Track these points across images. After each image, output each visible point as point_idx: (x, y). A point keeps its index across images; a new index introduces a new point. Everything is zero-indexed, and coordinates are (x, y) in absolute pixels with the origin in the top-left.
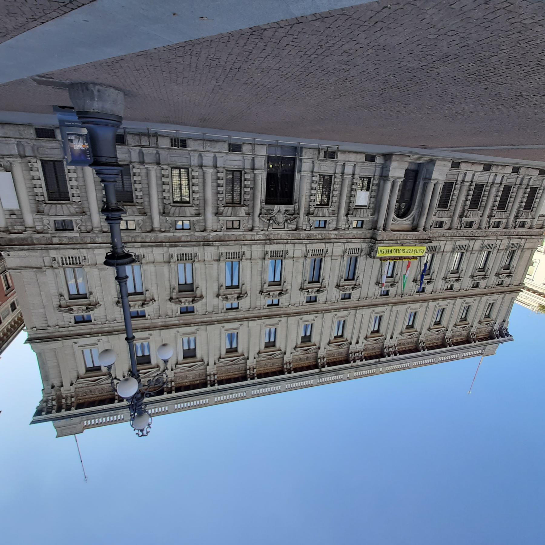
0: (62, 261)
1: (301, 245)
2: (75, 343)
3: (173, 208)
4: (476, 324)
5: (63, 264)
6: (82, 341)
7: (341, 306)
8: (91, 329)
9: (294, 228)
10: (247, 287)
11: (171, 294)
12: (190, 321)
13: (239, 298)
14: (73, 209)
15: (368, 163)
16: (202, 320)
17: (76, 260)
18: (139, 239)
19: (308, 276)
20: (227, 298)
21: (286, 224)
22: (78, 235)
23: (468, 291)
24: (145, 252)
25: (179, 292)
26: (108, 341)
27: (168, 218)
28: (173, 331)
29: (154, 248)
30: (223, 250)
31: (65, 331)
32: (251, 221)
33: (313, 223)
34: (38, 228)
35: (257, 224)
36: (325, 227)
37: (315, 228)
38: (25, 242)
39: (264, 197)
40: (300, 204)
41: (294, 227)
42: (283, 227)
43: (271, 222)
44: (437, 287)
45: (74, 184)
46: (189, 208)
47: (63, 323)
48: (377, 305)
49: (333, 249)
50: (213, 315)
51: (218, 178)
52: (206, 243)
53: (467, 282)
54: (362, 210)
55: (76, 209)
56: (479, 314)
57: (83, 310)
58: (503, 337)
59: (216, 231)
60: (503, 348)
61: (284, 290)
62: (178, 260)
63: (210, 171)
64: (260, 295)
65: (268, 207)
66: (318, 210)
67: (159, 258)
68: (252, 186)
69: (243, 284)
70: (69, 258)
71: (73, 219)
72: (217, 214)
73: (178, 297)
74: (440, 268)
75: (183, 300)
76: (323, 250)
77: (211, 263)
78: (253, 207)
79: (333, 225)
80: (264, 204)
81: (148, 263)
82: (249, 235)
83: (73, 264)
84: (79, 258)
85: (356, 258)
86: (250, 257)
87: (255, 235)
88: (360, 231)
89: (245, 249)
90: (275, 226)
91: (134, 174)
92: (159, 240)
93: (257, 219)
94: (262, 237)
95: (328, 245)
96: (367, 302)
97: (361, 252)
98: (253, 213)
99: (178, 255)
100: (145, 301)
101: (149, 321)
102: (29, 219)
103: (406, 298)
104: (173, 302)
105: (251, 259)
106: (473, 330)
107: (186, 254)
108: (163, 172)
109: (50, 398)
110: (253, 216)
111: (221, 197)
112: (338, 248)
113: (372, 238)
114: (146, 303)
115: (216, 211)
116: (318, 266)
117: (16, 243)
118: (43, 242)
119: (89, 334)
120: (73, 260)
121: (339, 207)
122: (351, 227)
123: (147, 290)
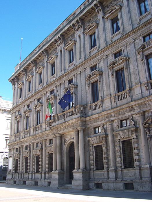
15: (100, 182)
36: (121, 121)
37: (128, 119)
40: (145, 138)
54: (96, 143)
58: (12, 80)
60: (12, 73)
66: (128, 135)
76: (119, 101)
116: (120, 85)
121: (114, 141)
122: (101, 126)
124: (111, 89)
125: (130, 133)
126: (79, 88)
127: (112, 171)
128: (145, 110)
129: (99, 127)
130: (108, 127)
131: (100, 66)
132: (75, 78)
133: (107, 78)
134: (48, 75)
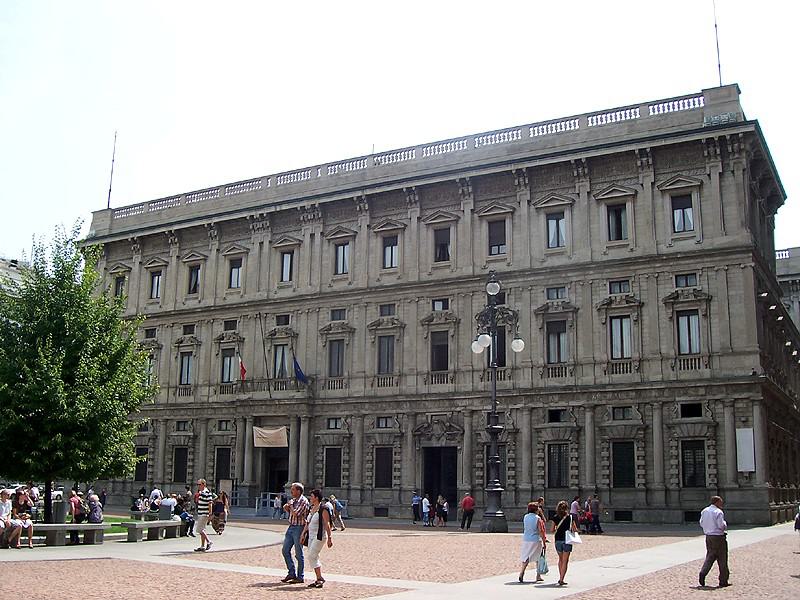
1: (408, 392)
4: (136, 268)
6: (690, 245)
14: (677, 432)
16: (536, 278)
18: (609, 396)
23: (158, 323)
25: (564, 322)
28: (574, 260)
29: (592, 383)
30: (508, 383)
32: (474, 424)
34: (721, 406)
35: (467, 420)
36: (379, 418)
38: (734, 388)
39: (459, 456)
41: (419, 418)
44: (208, 329)
45: (674, 462)
48: (291, 300)
51: (514, 477)
52: (531, 394)
53: (167, 337)
56: (134, 284)
63: (524, 485)
65: (453, 444)
67: (588, 370)
72: (516, 432)
74: (208, 359)
75: (560, 309)
78: (472, 443)
79: (367, 422)
81: (601, 363)
82: (477, 405)
86: (475, 373)
87: (469, 405)
88: (330, 414)
90: (444, 419)
91: (608, 476)
92: (586, 395)
95: (372, 393)
96: (306, 306)
101: (606, 276)
102: (726, 418)
103: (251, 312)
105: (473, 371)
106: (137, 258)
108: (576, 481)
109: (737, 156)
110: (472, 430)
111: (511, 454)
112: (358, 388)
113: (314, 405)
124: (367, 362)
126: (302, 340)
127: (356, 489)
129: (336, 419)
130: (356, 423)
131: (350, 317)
132: (295, 318)
134: (220, 280)
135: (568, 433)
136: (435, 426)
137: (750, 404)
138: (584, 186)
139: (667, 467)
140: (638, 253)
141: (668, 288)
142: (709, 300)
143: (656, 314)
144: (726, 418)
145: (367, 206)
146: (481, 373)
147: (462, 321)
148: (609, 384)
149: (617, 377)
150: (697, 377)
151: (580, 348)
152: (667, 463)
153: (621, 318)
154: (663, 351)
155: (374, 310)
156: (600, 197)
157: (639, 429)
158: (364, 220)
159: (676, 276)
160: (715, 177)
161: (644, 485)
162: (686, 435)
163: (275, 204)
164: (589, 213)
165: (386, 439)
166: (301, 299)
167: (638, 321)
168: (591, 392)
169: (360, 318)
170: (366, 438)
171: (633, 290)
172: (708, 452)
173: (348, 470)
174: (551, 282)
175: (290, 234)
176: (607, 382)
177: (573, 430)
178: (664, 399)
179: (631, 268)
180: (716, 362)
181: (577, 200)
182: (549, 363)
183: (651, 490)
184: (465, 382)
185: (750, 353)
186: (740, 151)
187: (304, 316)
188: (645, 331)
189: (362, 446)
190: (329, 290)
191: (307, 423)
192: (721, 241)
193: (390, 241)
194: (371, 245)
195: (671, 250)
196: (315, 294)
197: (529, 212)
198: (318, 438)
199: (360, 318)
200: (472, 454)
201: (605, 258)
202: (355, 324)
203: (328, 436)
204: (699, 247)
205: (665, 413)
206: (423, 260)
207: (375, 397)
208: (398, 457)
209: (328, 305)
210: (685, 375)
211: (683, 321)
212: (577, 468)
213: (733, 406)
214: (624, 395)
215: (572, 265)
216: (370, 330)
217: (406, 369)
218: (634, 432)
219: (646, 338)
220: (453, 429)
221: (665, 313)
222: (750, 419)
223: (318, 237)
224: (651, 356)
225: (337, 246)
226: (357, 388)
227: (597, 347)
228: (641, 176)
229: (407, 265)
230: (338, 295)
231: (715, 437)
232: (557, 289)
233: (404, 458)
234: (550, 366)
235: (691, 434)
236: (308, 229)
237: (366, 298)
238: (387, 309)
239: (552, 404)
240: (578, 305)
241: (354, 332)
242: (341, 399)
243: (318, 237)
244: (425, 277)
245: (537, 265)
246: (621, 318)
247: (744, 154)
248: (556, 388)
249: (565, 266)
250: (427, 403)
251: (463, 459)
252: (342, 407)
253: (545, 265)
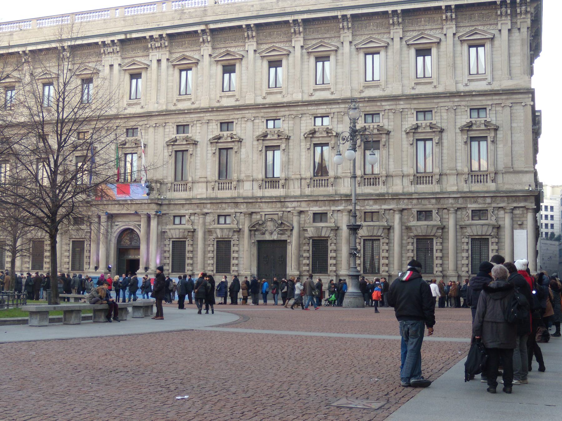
0: (487, 179)
1: (245, 195)
2: (489, 84)
3: (379, 234)
5: (487, 175)
6: (482, 86)
7: (187, 116)
8: (471, 100)
9: (254, 214)
10: (304, 145)
11: (389, 139)
12: (369, 104)
13: (313, 132)
17: (475, 179)
18: (415, 201)
19: (233, 159)
20: (327, 133)
21: (263, 219)
22: (469, 206)
24: (410, 188)
26: (457, 83)
27: (386, 224)
29: (401, 192)
30: (330, 190)
31: (496, 99)
32: (302, 222)
33: (233, 220)
36: (219, 216)
37: (230, 215)
38: (514, 198)
41: (254, 216)
42: (267, 216)
43: (280, 222)
45: (465, 254)
46: (364, 235)
47: (497, 109)
49: (207, 190)
50: (343, 110)
51: (335, 265)
52: (347, 198)
55: (465, 231)
57: (475, 124)
59: (338, 211)
61: (261, 141)
62: (379, 178)
64: (290, 135)
65: (283, 238)
67: (397, 181)
68: (301, 259)
69: (308, 149)
70: (481, 181)
71: (470, 222)
73: (380, 136)
76: (219, 189)
77: (344, 175)
79: (209, 219)
80: (288, 241)
81: (408, 176)
82: (304, 207)
83: (478, 175)
84: (472, 182)
85: (175, 180)
89: (308, 191)
90: (275, 217)
92: (395, 200)
93: (295, 225)
94: (289, 204)
95: (213, 195)
97: (171, 187)
98: (300, 231)
99: (379, 184)
100: (414, 133)
101: (413, 106)
102: (507, 222)
104: (385, 130)
105: (301, 179)
107: (370, 184)
108: (387, 269)
109: (523, 16)
110: (299, 227)
112: (200, 191)
114: (413, 131)
115: (338, 231)
117: (521, 198)
118: (499, 198)
119: (473, 95)
120: (478, 179)
123: (412, 144)
124: (209, 170)
125: (231, 234)
126: (150, 150)
128: (254, 210)
133: (205, 154)
135: (381, 231)
136: (269, 223)
137: (525, 211)
138: (397, 32)
139: (460, 259)
140: (440, 89)
141: (464, 119)
142: (496, 130)
143: (453, 139)
144: (507, 222)
145: (209, 38)
146: (308, 181)
147: (292, 138)
148: (415, 193)
149: (422, 188)
150: (485, 189)
151: (391, 163)
152: (459, 255)
153: (425, 140)
154: (459, 168)
155: (215, 127)
156: (411, 42)
157: (438, 228)
158: (206, 50)
159: (471, 109)
160: (505, 33)
161: (441, 272)
162: (476, 234)
163: (125, 33)
164: (401, 54)
165: (226, 234)
166: (149, 115)
167: (439, 143)
168: (400, 199)
169: (203, 132)
170: (208, 232)
171: (436, 119)
172: (491, 247)
173: (192, 258)
174: (368, 109)
175: (138, 59)
176: (413, 191)
177: (384, 228)
178: (459, 206)
179: (435, 101)
180: (500, 178)
181: (391, 43)
182: (365, 174)
183: (446, 276)
184: (294, 188)
185: (527, 172)
186: (527, 12)
187: (151, 130)
188: (445, 151)
189: (205, 239)
190: (173, 108)
191: (156, 220)
192: (507, 84)
193: (229, 69)
194: (212, 72)
195: (467, 89)
196: (162, 111)
197: (350, 51)
198: (164, 232)
199: (203, 132)
200: (300, 246)
201: (413, 92)
202: (197, 138)
203: (175, 231)
204: (489, 88)
205: (459, 216)
206: (258, 86)
207: (216, 198)
208: (236, 248)
209: (173, 121)
210: (477, 187)
211: (475, 144)
212: (387, 258)
213: (512, 213)
214: (426, 202)
215: (385, 97)
216: (211, 143)
217: (242, 176)
218: (434, 231)
219: (445, 158)
220: (283, 226)
221: (461, 138)
222: (525, 223)
223: (164, 63)
224: (448, 172)
225: (181, 71)
226: (200, 191)
227: (405, 163)
228: (445, 27)
229: (244, 90)
230: (182, 112)
231: (498, 236)
232: (373, 115)
233: (241, 249)
234: (366, 177)
235: (480, 234)
236: (154, 55)
237: (208, 116)
238: (226, 125)
239: (367, 207)
240: (390, 128)
241: (196, 144)
242: (186, 199)
243: (164, 63)
244: (260, 101)
245: (356, 95)
246: (425, 140)
247: (529, 16)
248: (371, 195)
249: (380, 97)
250: (261, 204)
251: (292, 250)
252: (187, 207)
253: (363, 95)
